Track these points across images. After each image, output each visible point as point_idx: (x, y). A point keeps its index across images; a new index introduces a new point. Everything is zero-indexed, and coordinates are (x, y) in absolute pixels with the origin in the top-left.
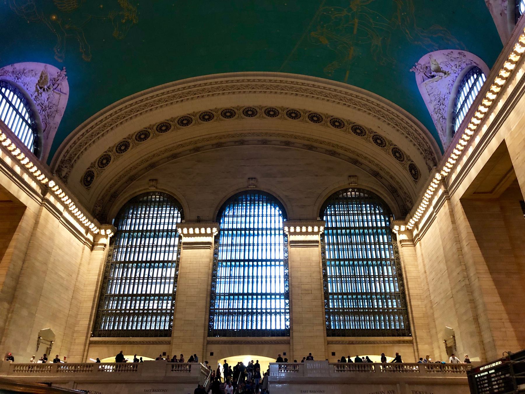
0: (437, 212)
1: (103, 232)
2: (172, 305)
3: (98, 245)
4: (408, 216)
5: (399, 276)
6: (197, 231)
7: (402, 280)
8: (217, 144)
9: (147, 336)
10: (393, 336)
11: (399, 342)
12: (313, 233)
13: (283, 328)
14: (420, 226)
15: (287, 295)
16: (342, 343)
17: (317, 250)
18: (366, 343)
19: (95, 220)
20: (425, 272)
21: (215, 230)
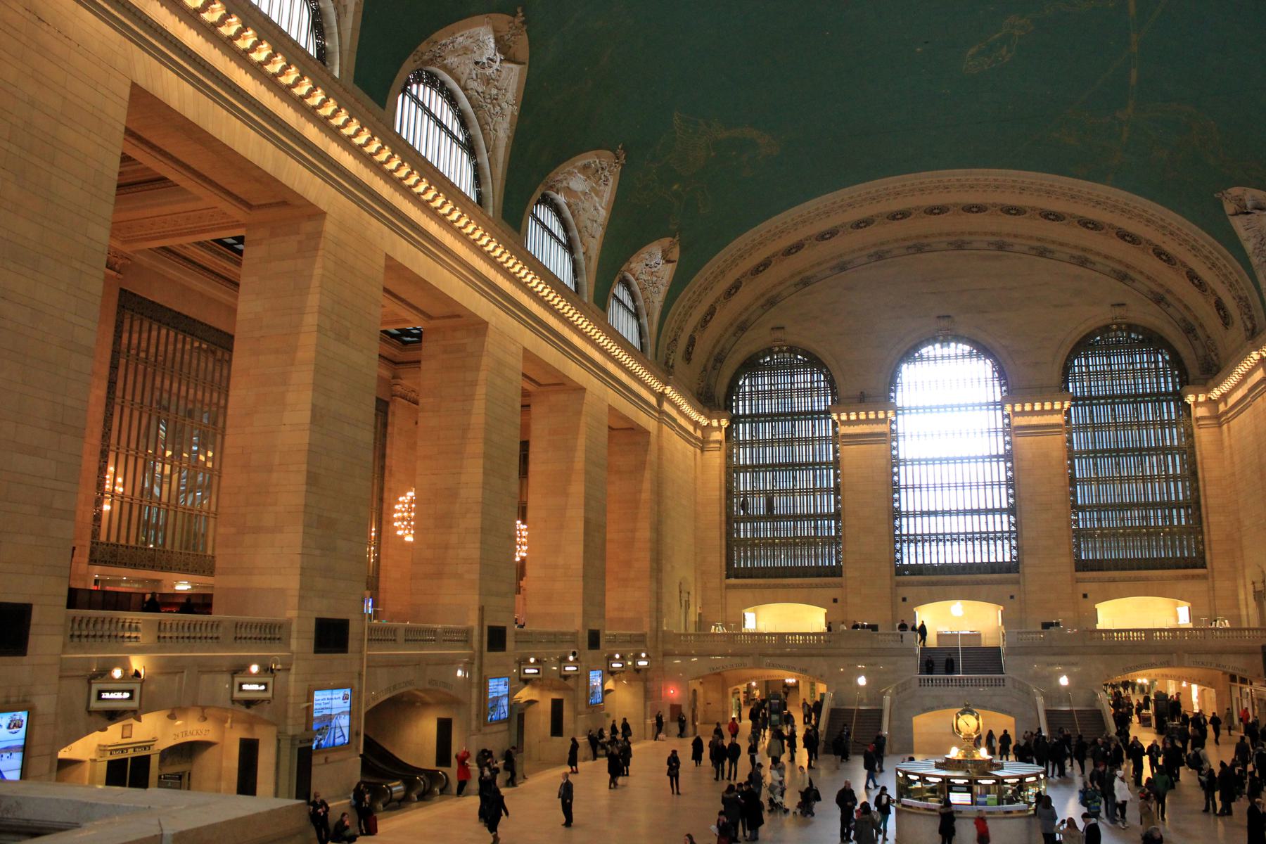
0: (1254, 399)
1: (715, 423)
2: (837, 530)
3: (709, 442)
4: (1211, 383)
5: (1192, 474)
6: (862, 416)
7: (1197, 480)
8: (876, 253)
9: (805, 576)
10: (1178, 567)
11: (1186, 577)
12: (1052, 412)
13: (1007, 559)
14: (1232, 400)
15: (1011, 510)
16: (1100, 581)
17: (1058, 441)
18: (1136, 579)
19: (706, 410)
20: (1233, 474)
21: (890, 414)
